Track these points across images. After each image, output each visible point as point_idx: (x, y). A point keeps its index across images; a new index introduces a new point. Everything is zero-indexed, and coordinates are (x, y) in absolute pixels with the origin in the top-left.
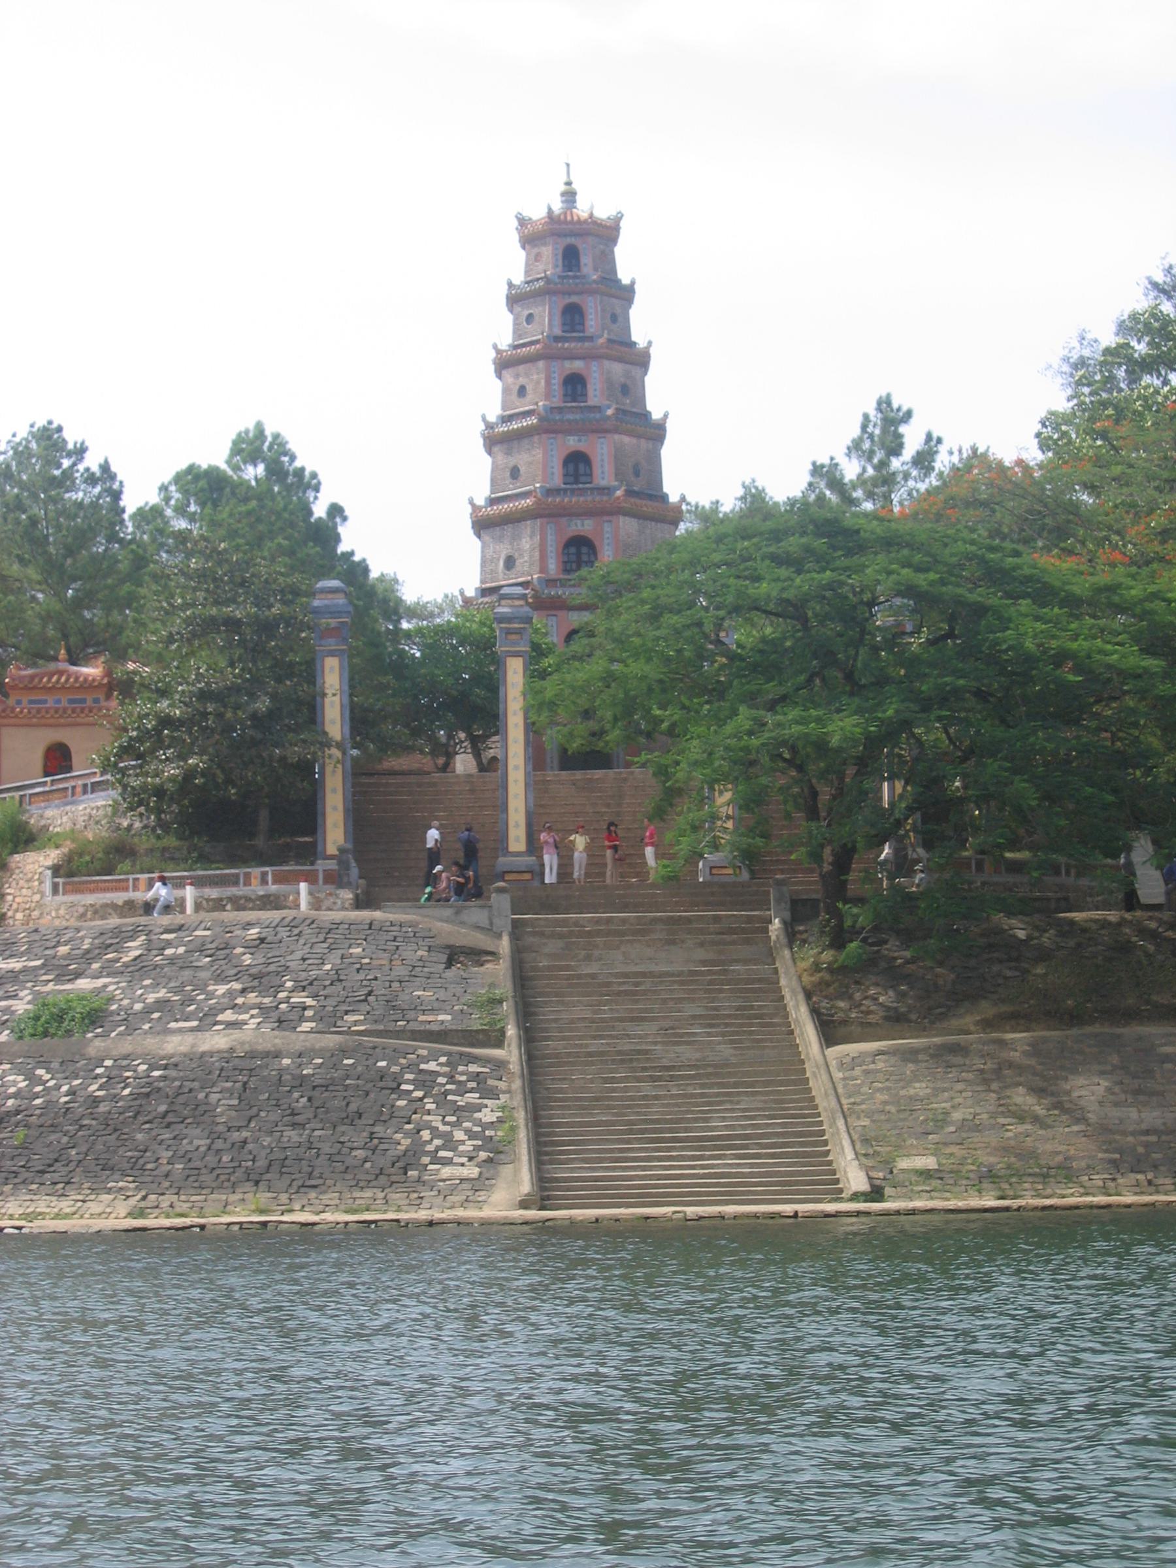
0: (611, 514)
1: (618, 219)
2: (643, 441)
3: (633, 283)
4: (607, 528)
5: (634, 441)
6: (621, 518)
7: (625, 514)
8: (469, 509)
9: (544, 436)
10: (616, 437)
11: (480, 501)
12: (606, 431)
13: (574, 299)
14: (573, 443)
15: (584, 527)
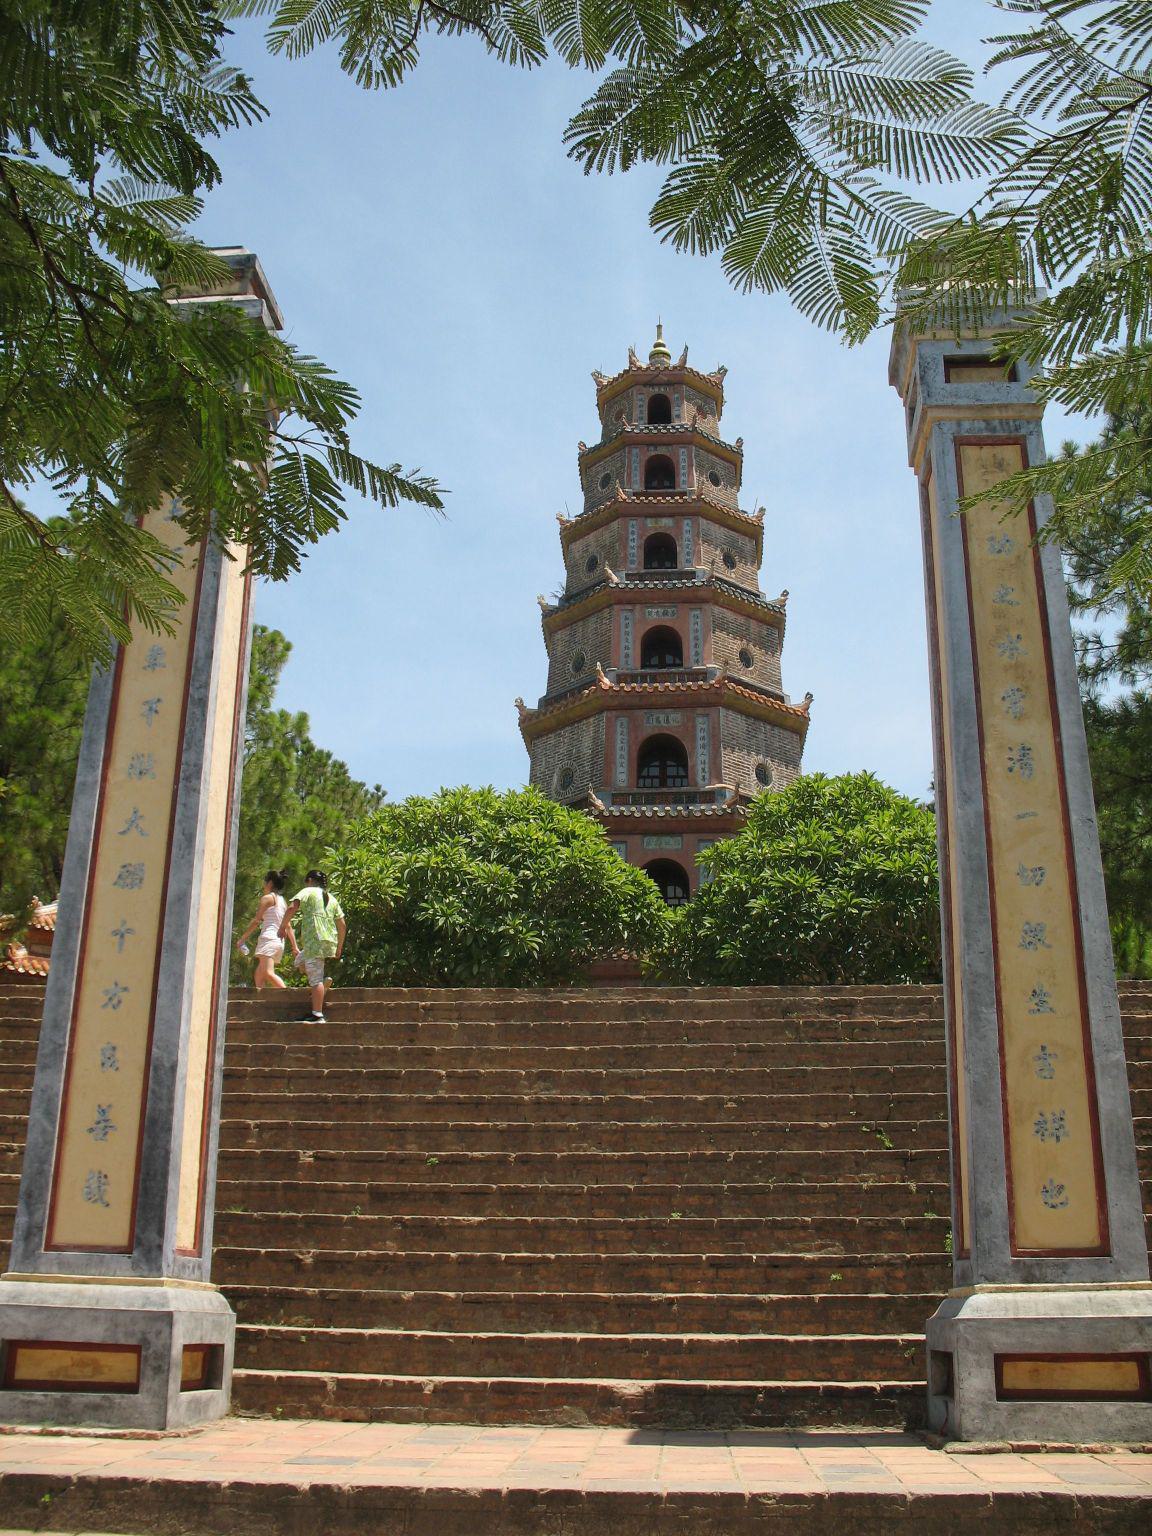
0: (709, 705)
1: (723, 371)
2: (753, 624)
3: (740, 441)
4: (701, 723)
5: (741, 620)
6: (723, 711)
7: (728, 707)
8: (516, 715)
9: (616, 607)
10: (717, 609)
11: (532, 704)
12: (705, 601)
13: (662, 451)
14: (655, 616)
15: (669, 722)
